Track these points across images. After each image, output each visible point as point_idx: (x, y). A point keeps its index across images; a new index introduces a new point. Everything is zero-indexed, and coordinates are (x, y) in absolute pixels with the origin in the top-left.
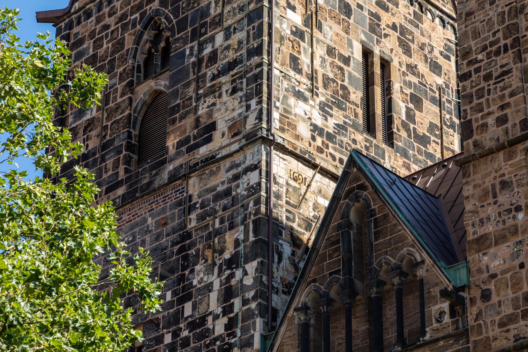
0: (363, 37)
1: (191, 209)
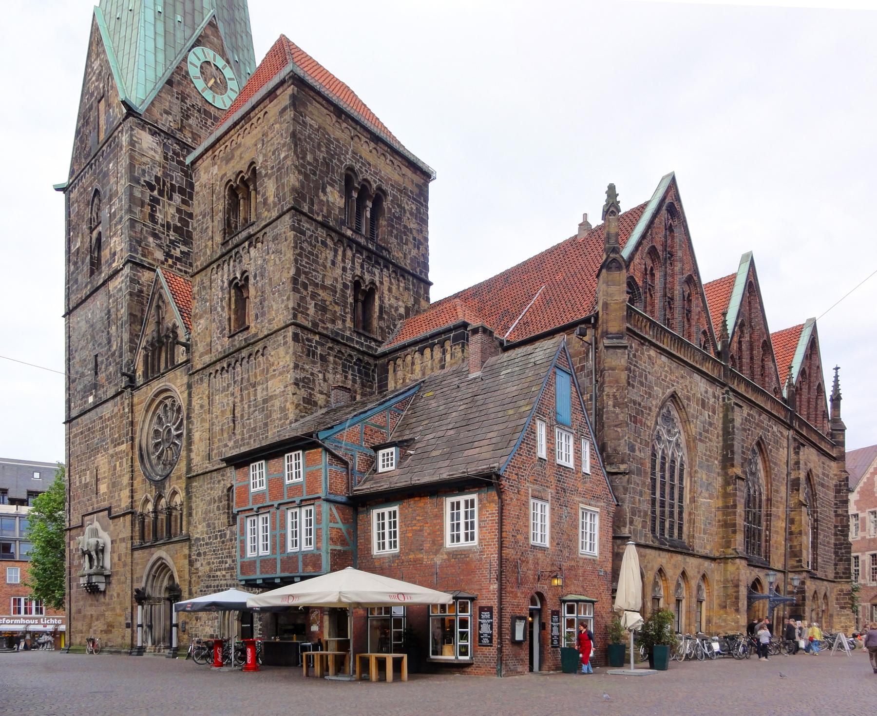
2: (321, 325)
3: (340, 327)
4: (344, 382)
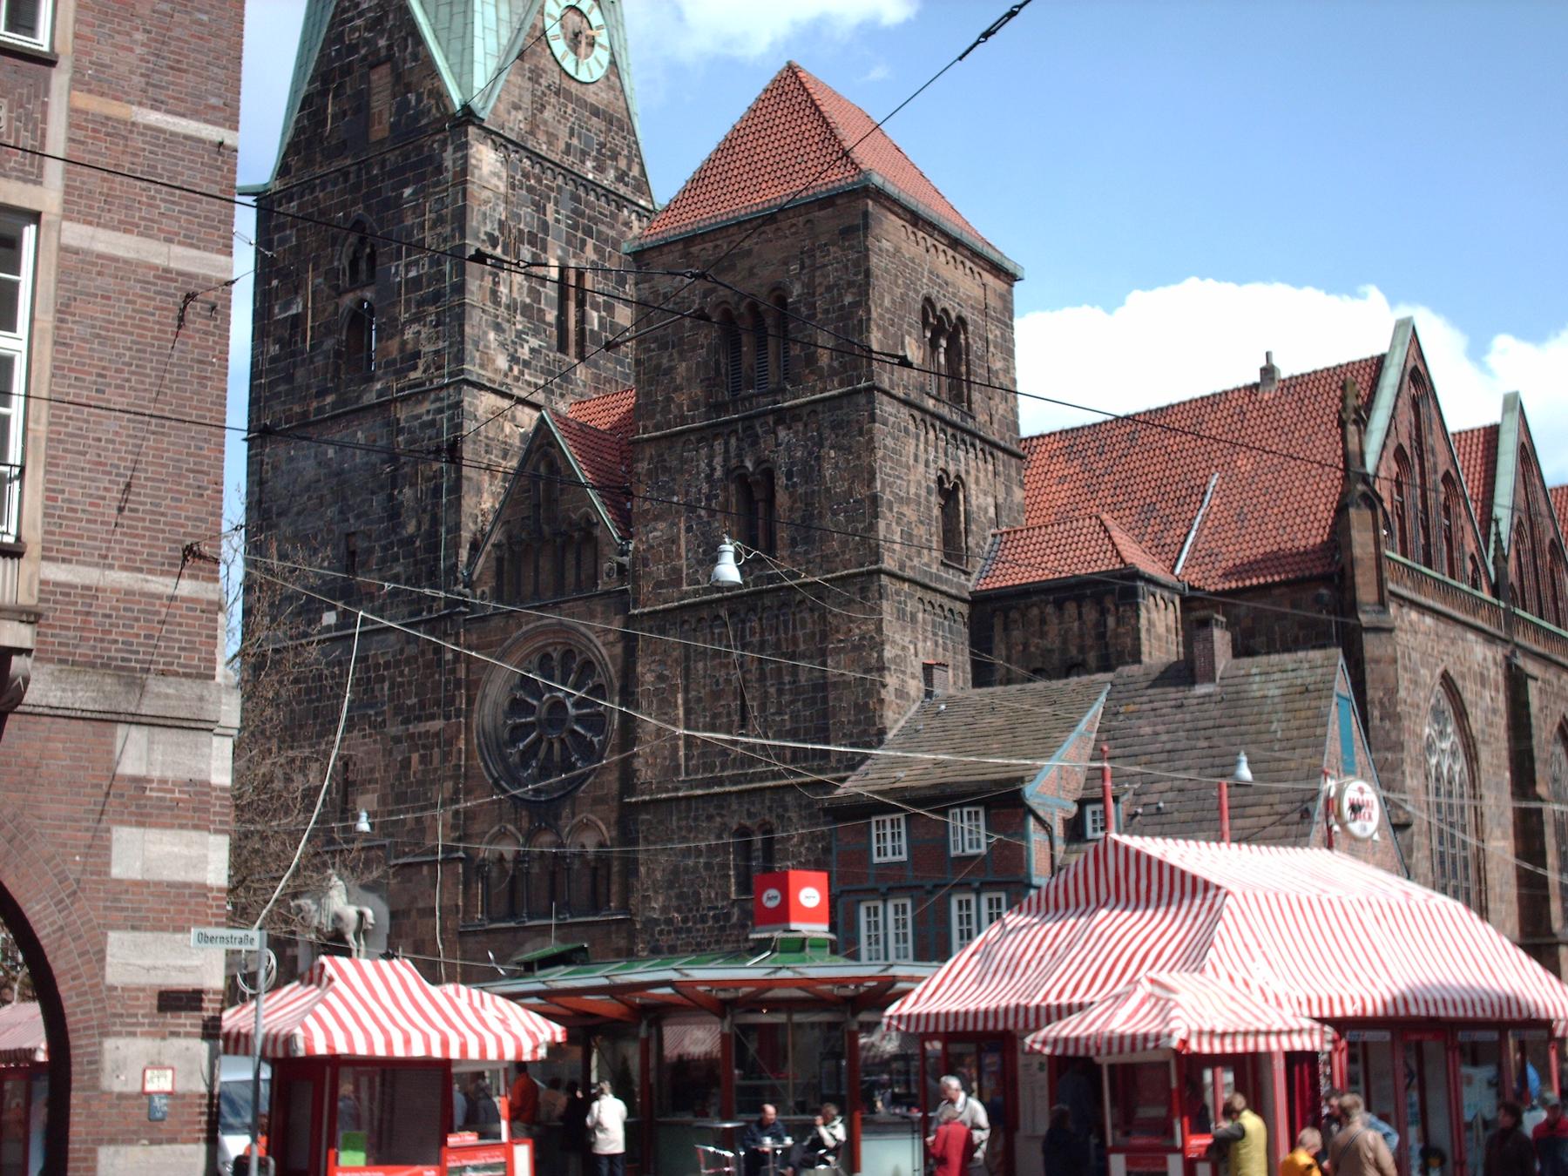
0: (559, 252)
1: (400, 431)
2: (908, 563)
3: (926, 560)
4: (935, 654)
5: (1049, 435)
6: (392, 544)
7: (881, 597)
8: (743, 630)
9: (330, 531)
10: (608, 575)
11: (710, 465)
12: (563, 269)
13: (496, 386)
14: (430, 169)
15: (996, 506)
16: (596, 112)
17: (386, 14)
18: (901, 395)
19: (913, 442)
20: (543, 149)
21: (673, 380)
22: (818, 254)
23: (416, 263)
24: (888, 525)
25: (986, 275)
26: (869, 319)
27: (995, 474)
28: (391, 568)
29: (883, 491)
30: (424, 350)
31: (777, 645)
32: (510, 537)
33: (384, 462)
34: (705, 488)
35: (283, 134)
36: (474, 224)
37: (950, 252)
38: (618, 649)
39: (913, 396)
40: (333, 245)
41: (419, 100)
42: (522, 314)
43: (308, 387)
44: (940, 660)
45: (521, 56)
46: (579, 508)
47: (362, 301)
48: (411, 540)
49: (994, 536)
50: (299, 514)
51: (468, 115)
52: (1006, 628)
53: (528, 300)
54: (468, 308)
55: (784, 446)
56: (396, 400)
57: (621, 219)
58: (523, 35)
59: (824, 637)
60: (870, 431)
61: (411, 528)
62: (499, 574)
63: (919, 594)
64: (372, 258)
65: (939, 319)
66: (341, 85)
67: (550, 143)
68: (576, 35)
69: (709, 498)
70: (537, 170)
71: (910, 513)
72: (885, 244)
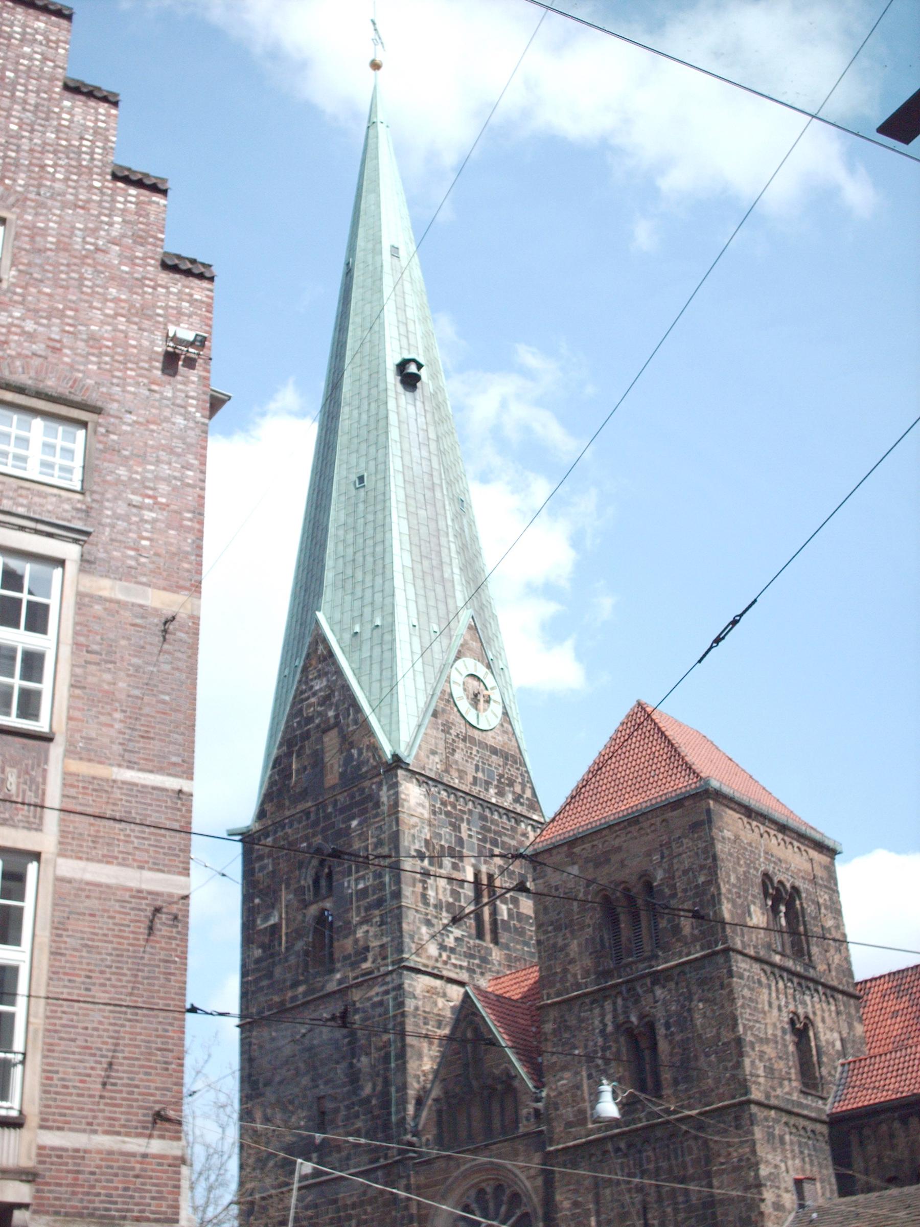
2: (773, 1093)
3: (787, 1089)
5: (880, 977)
6: (353, 1104)
7: (752, 1124)
8: (641, 1159)
9: (305, 1096)
10: (528, 1119)
11: (602, 1021)
12: (477, 875)
13: (429, 970)
14: (371, 804)
15: (842, 1040)
16: (494, 751)
17: (333, 691)
18: (752, 952)
19: (766, 991)
20: (456, 783)
21: (567, 955)
22: (674, 845)
23: (363, 877)
24: (753, 1063)
25: (811, 851)
26: (719, 894)
27: (838, 1013)
28: (353, 1124)
29: (745, 1033)
30: (372, 945)
31: (670, 1170)
32: (446, 1093)
33: (345, 1037)
34: (600, 1041)
35: (261, 787)
36: (406, 844)
37: (780, 836)
38: (539, 1181)
39: (762, 953)
40: (300, 868)
41: (360, 753)
42: (447, 911)
43: (285, 980)
44: (808, 1174)
45: (435, 714)
46: (500, 1064)
47: (323, 910)
48: (368, 1100)
49: (843, 1065)
50: (280, 1083)
51: (398, 761)
52: (861, 1142)
53: (451, 900)
54: (404, 909)
55: (661, 1002)
56: (351, 986)
57: (519, 831)
58: (436, 698)
59: (708, 1160)
60: (730, 985)
61: (368, 1090)
62: (439, 1124)
63: (784, 1119)
64: (330, 875)
65: (777, 890)
66: (302, 747)
67: (461, 778)
68: (476, 695)
69: (604, 1049)
70: (452, 798)
71: (770, 1051)
72: (727, 834)
